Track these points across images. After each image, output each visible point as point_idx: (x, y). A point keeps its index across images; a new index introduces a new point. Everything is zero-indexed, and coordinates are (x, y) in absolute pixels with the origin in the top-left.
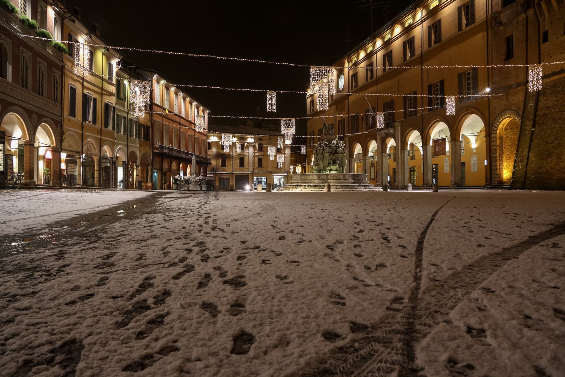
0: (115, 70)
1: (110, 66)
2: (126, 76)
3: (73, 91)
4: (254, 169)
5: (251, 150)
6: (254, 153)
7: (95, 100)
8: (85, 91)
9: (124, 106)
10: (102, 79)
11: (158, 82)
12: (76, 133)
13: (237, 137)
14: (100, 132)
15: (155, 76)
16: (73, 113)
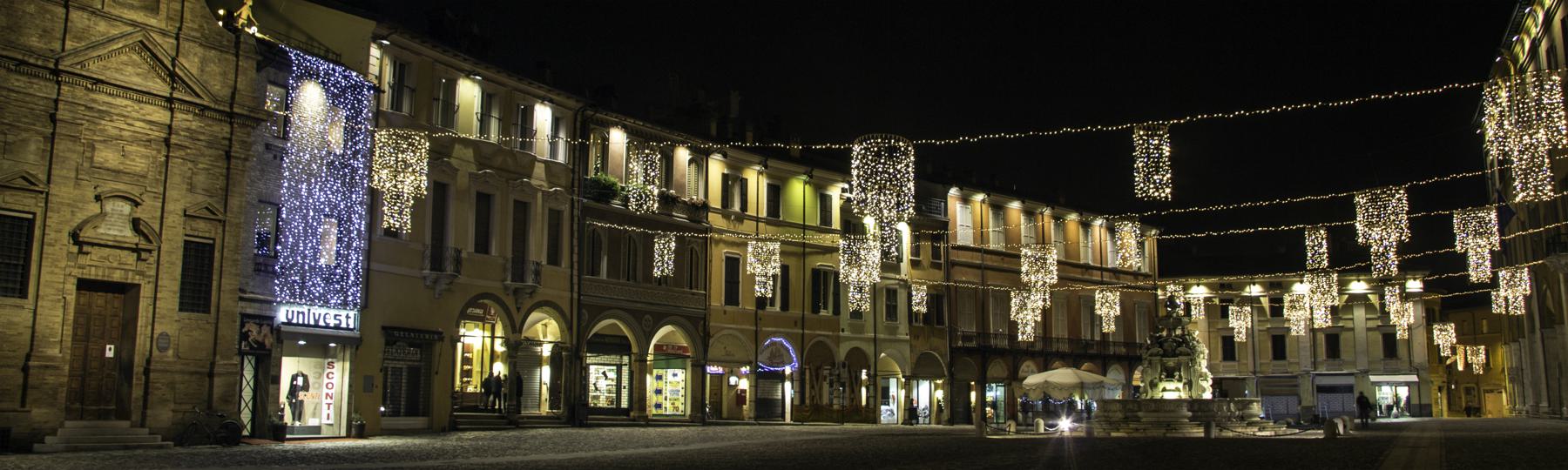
0: (836, 205)
1: (825, 201)
4: (1315, 365)
10: (804, 227)
12: (742, 331)
13: (1261, 284)
14: (802, 322)
15: (953, 191)
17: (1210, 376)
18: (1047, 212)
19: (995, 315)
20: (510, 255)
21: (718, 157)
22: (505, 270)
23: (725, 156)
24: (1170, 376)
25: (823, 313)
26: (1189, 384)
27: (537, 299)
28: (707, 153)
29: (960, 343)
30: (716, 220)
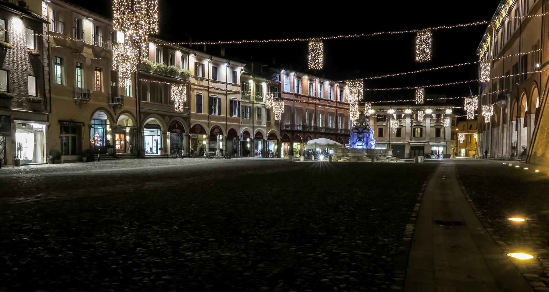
0: (239, 75)
1: (234, 74)
2: (251, 77)
3: (199, 97)
5: (408, 120)
6: (412, 123)
7: (219, 99)
8: (211, 95)
9: (249, 98)
11: (287, 75)
13: (394, 109)
15: (283, 71)
16: (199, 109)
17: (374, 141)
18: (318, 80)
19: (297, 118)
20: (110, 93)
21: (193, 55)
22: (109, 99)
23: (195, 55)
24: (360, 140)
25: (234, 116)
26: (367, 143)
27: (122, 110)
28: (188, 54)
29: (284, 128)
30: (192, 80)
